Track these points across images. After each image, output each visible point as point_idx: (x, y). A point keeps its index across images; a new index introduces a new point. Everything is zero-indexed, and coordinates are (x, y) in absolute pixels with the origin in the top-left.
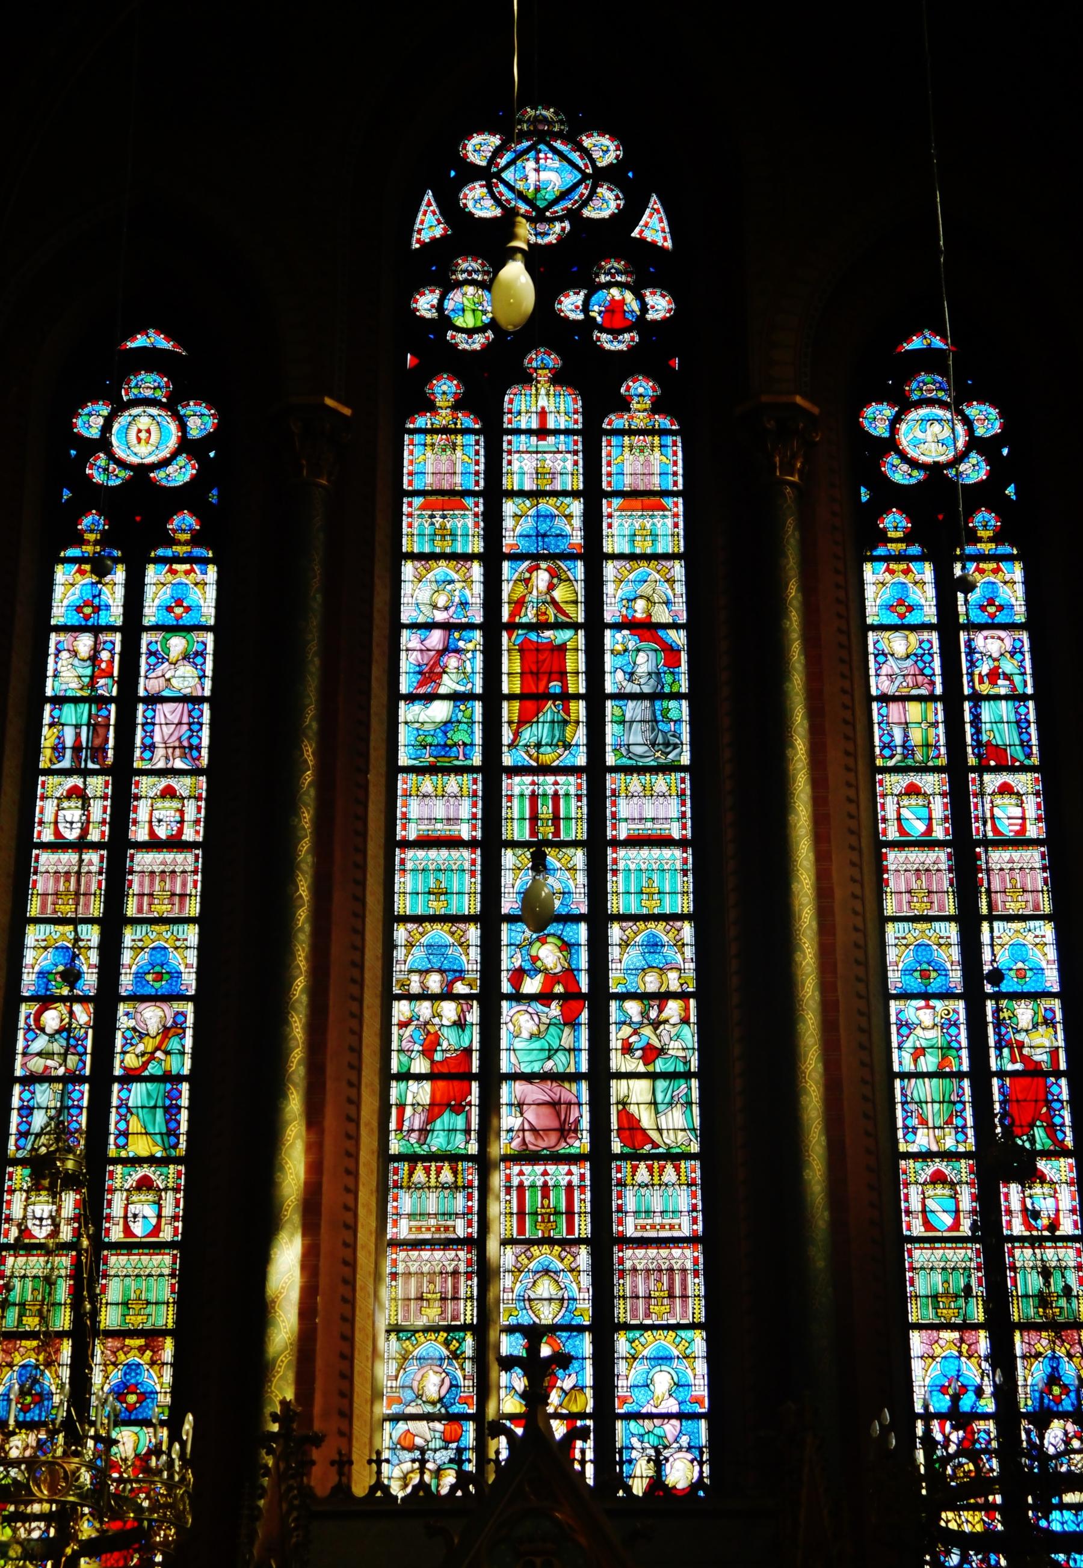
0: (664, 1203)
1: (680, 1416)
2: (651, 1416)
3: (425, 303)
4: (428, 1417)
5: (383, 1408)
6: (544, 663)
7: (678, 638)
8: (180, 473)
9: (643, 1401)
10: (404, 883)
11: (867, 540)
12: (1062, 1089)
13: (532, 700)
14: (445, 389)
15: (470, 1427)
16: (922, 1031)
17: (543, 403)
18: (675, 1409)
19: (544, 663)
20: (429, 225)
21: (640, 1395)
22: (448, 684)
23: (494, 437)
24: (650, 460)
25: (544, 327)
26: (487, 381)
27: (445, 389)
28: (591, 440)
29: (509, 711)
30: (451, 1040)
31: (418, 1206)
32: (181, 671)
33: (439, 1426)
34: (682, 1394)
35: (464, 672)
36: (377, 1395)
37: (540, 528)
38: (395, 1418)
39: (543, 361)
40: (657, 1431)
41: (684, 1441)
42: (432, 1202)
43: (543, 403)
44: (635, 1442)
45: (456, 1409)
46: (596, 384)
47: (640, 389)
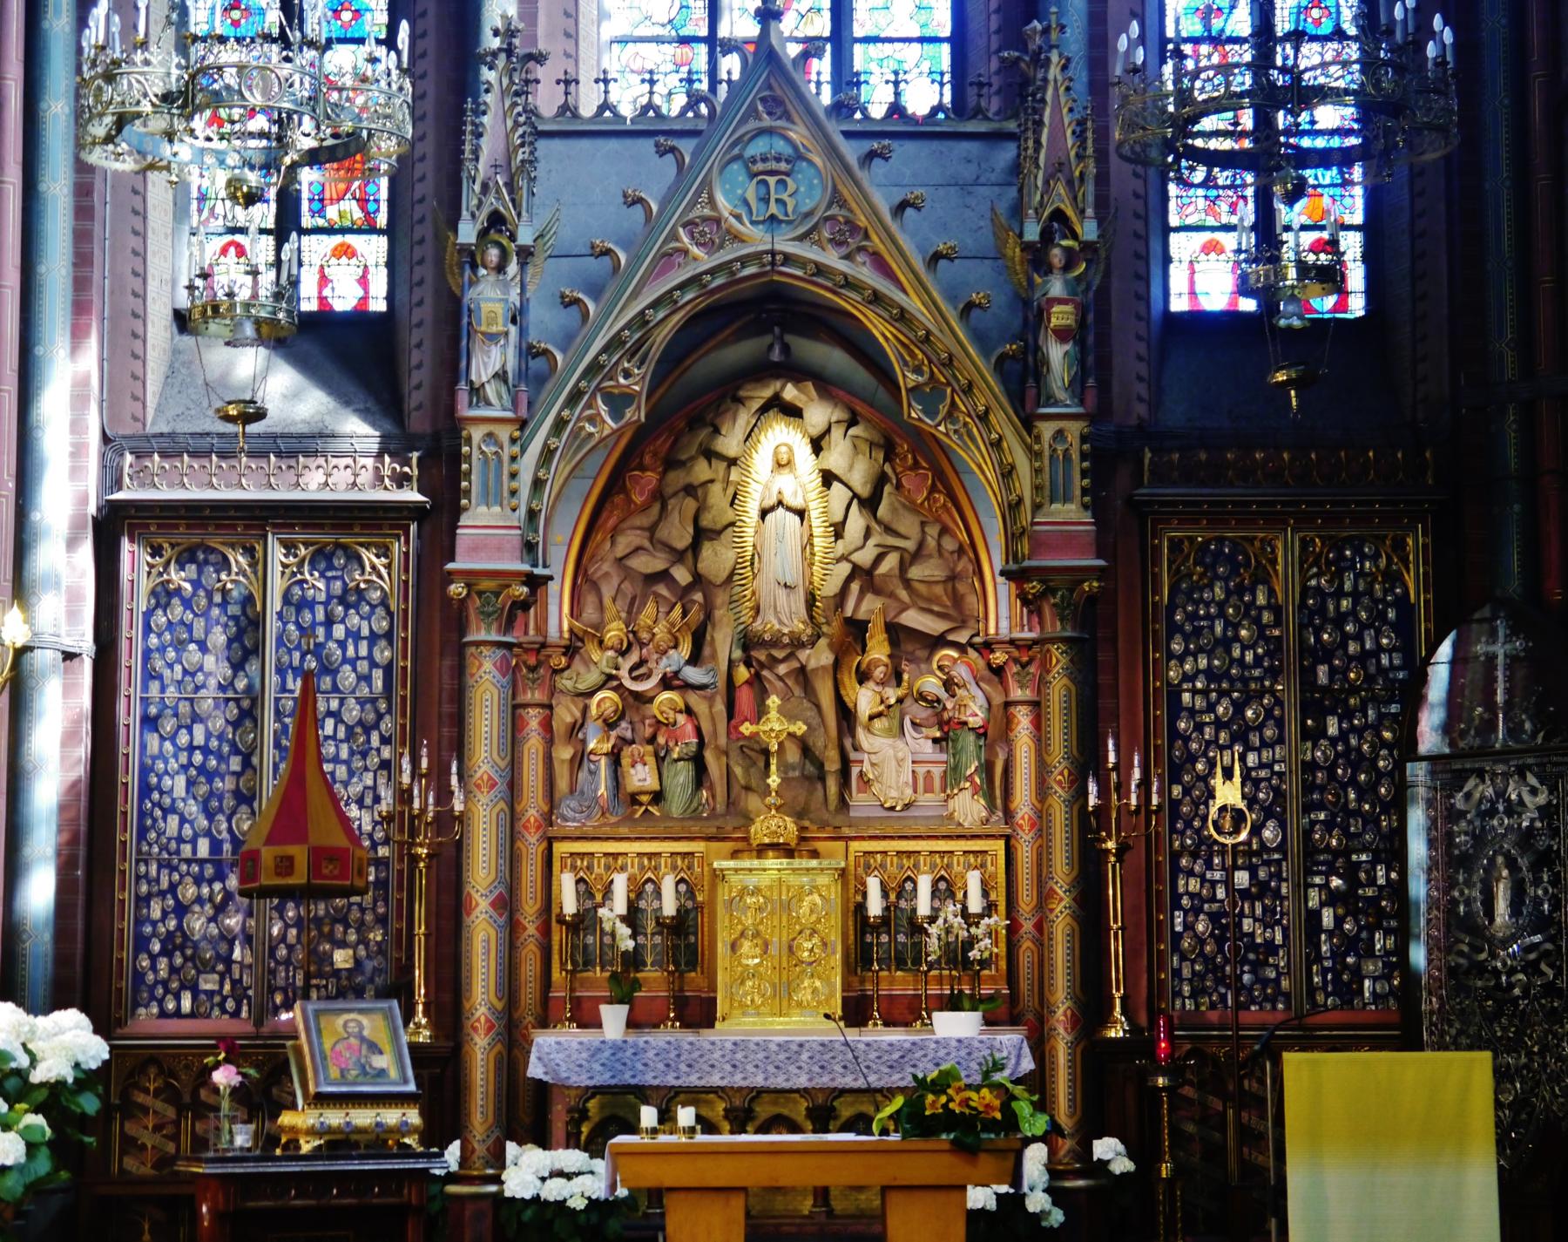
1: (922, 40)
2: (891, 40)
4: (658, 40)
5: (609, 30)
9: (883, 23)
15: (702, 49)
18: (916, 34)
21: (881, 17)
33: (669, 49)
34: (923, 16)
36: (603, 15)
38: (623, 41)
40: (897, 56)
41: (925, 67)
44: (873, 67)
45: (684, 32)
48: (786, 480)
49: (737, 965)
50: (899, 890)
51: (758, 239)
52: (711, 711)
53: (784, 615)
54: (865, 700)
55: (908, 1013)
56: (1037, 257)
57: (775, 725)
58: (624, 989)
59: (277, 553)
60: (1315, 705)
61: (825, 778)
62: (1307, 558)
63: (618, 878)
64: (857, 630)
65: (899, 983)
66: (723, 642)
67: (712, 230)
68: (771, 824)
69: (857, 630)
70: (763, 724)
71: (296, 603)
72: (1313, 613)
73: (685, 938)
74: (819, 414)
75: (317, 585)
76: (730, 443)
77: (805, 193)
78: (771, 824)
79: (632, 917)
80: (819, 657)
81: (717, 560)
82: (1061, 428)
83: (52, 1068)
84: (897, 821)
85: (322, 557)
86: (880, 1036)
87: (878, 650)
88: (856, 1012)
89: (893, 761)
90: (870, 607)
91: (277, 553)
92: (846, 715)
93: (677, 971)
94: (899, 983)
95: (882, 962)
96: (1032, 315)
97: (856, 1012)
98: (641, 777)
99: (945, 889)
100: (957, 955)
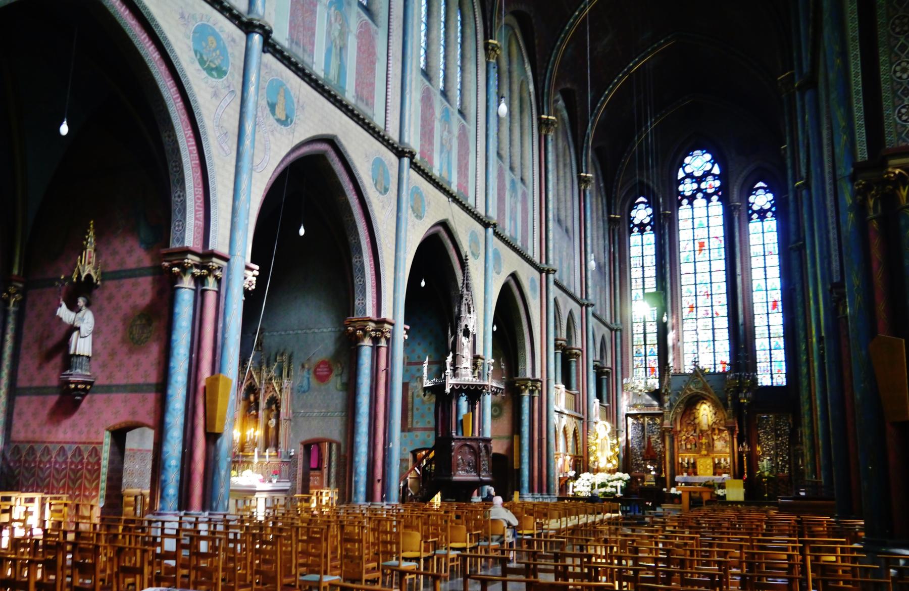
0: (723, 323)
3: (681, 188)
6: (702, 245)
7: (722, 239)
8: (647, 220)
10: (683, 280)
11: (750, 219)
12: (780, 303)
13: (701, 250)
14: (685, 202)
16: (758, 298)
17: (700, 202)
19: (702, 245)
20: (681, 175)
22: (688, 249)
23: (692, 208)
24: (717, 208)
25: (699, 190)
26: (691, 199)
27: (685, 202)
28: (707, 206)
29: (697, 253)
30: (691, 304)
31: (688, 326)
32: (650, 251)
35: (690, 247)
37: (700, 222)
39: (699, 195)
42: (690, 325)
43: (700, 202)
46: (708, 197)
47: (715, 198)
48: (705, 413)
49: (700, 468)
50: (720, 460)
51: (695, 390)
52: (697, 439)
53: (705, 428)
54: (715, 437)
55: (720, 474)
56: (726, 392)
57: (704, 441)
58: (686, 472)
59: (646, 419)
60: (777, 436)
61: (710, 446)
62: (776, 418)
63: (685, 458)
64: (713, 430)
65: (720, 471)
66: (698, 431)
67: (690, 390)
68: (704, 452)
69: (713, 430)
70: (703, 441)
71: (649, 424)
72: (776, 424)
73: (694, 465)
74: (708, 404)
75: (651, 422)
76: (698, 407)
77: (700, 385)
78: (704, 452)
79: (688, 463)
80: (709, 432)
81: (697, 421)
82: (730, 411)
83: (625, 479)
84: (720, 452)
85: (651, 419)
86: (717, 477)
87: (717, 432)
88: (714, 474)
89: (719, 445)
90: (715, 426)
91: (646, 419)
92: (713, 439)
93: (692, 468)
94: (720, 471)
95: (717, 469)
96: (726, 399)
97: (714, 474)
98: (689, 446)
99: (725, 460)
100: (725, 467)
